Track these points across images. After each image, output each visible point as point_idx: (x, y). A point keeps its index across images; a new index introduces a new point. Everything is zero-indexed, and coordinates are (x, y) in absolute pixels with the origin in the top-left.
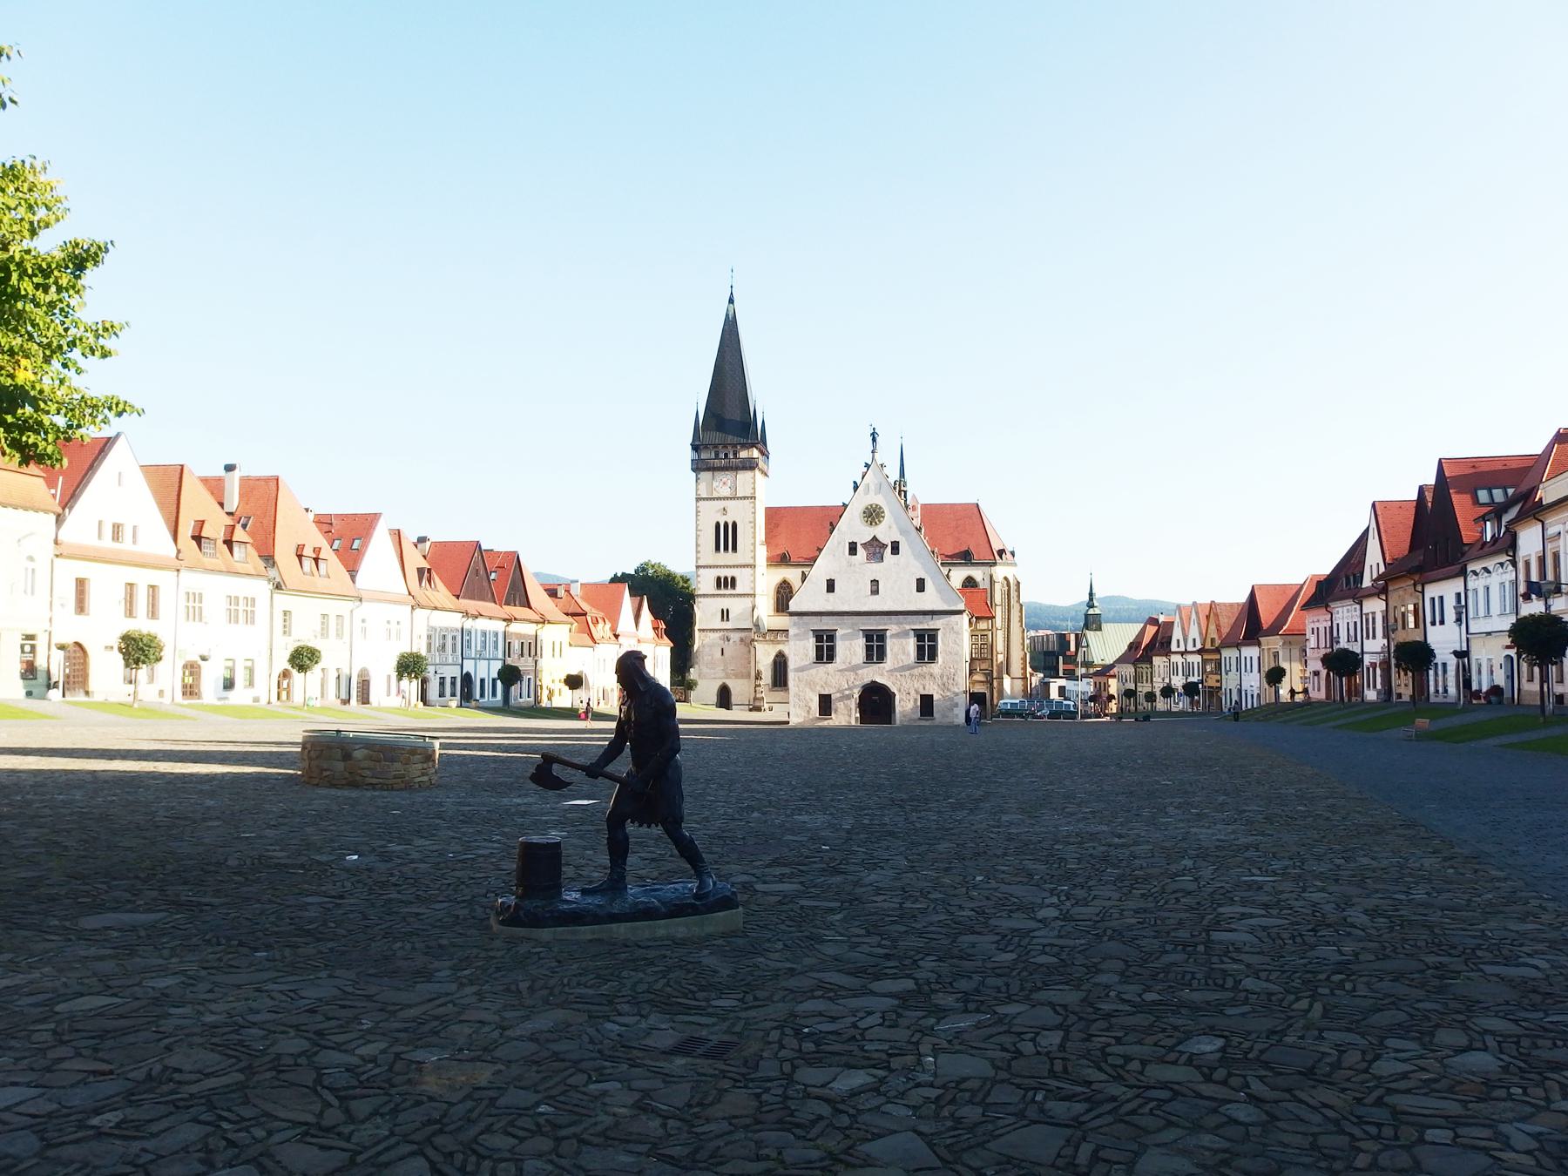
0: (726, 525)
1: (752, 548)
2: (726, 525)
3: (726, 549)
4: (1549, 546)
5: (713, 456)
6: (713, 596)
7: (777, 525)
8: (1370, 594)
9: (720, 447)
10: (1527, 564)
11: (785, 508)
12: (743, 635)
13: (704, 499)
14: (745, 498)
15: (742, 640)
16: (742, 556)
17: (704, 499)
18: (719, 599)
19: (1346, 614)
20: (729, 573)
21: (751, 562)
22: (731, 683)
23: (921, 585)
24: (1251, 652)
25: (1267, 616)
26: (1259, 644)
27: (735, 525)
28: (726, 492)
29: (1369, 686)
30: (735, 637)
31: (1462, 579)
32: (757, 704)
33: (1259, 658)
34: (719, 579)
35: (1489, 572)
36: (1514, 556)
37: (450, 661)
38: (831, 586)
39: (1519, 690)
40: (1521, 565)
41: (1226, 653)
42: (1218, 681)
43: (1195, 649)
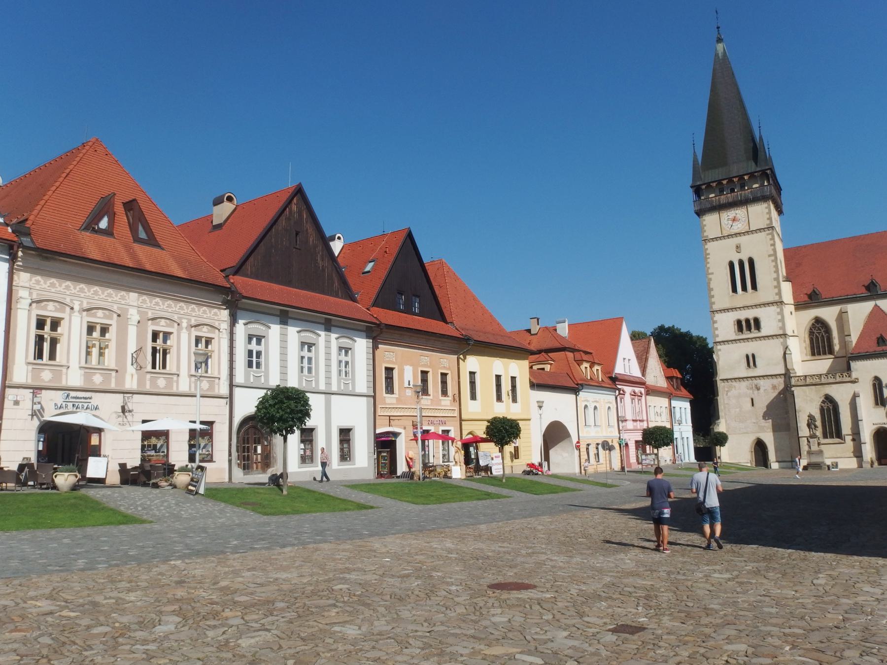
1: (775, 283)
2: (741, 263)
3: (744, 288)
6: (735, 340)
9: (725, 182)
11: (805, 247)
13: (716, 239)
14: (760, 230)
15: (774, 387)
16: (766, 291)
17: (716, 239)
18: (742, 344)
20: (750, 314)
21: (777, 298)
27: (751, 262)
28: (738, 227)
30: (764, 384)
32: (815, 459)
34: (739, 322)
37: (184, 385)
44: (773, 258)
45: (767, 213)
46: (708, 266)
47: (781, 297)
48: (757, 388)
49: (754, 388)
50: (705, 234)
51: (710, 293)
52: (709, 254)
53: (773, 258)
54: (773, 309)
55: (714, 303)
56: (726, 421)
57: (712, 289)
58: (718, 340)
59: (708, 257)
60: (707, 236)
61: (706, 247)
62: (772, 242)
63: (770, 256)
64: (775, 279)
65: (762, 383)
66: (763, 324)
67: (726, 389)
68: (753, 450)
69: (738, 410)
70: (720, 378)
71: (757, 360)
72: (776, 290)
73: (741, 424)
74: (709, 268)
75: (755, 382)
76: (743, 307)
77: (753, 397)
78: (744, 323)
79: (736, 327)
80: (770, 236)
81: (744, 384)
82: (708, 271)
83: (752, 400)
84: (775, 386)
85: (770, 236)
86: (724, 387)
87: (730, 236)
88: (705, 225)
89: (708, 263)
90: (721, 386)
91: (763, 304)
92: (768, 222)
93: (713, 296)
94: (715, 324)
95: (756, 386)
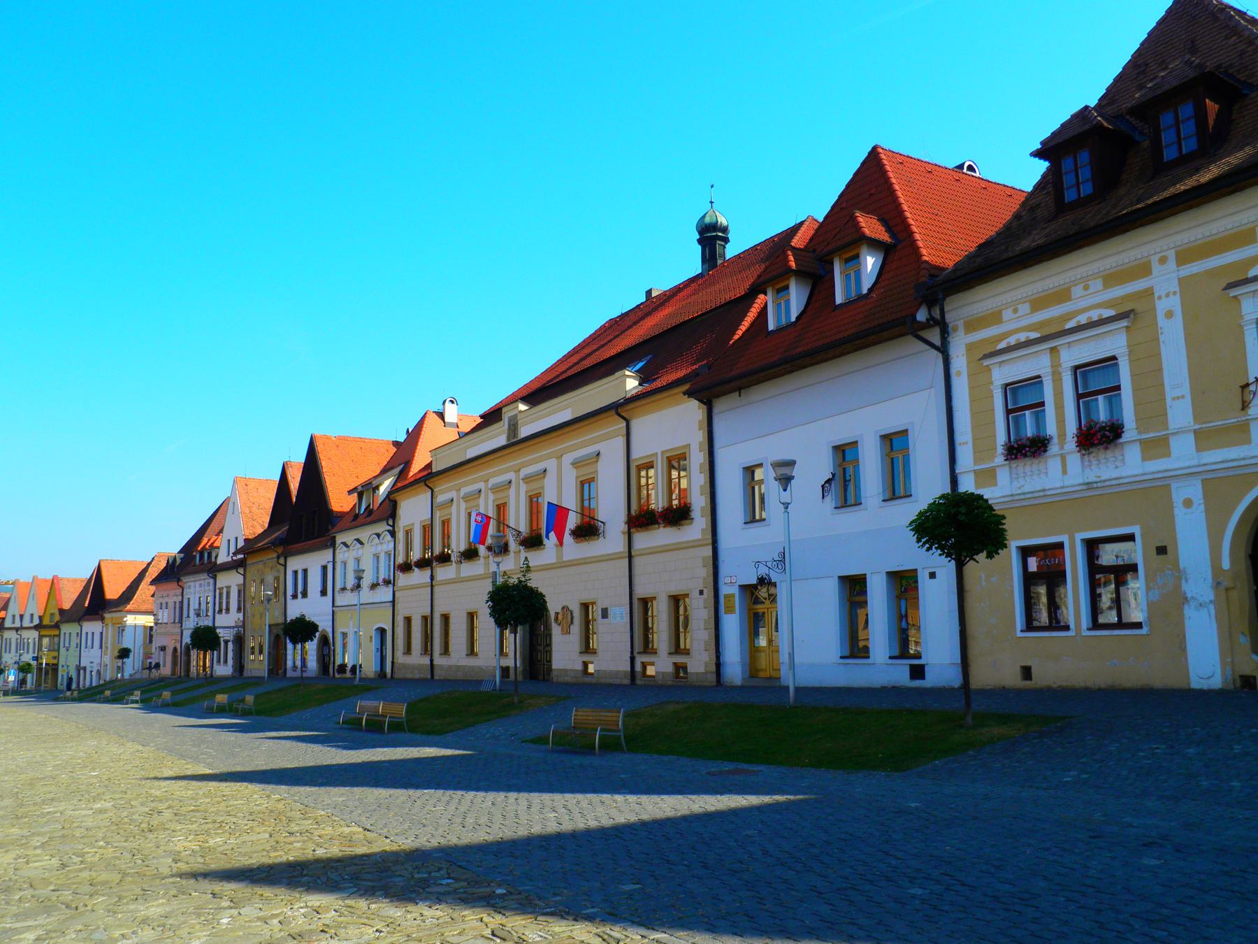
4: (438, 514)
8: (227, 567)
10: (408, 533)
19: (198, 588)
24: (93, 627)
25: (113, 590)
26: (102, 619)
29: (219, 661)
31: (331, 550)
33: (102, 633)
35: (361, 543)
36: (393, 526)
39: (393, 663)
40: (400, 535)
41: (67, 629)
42: (55, 658)
43: (32, 625)
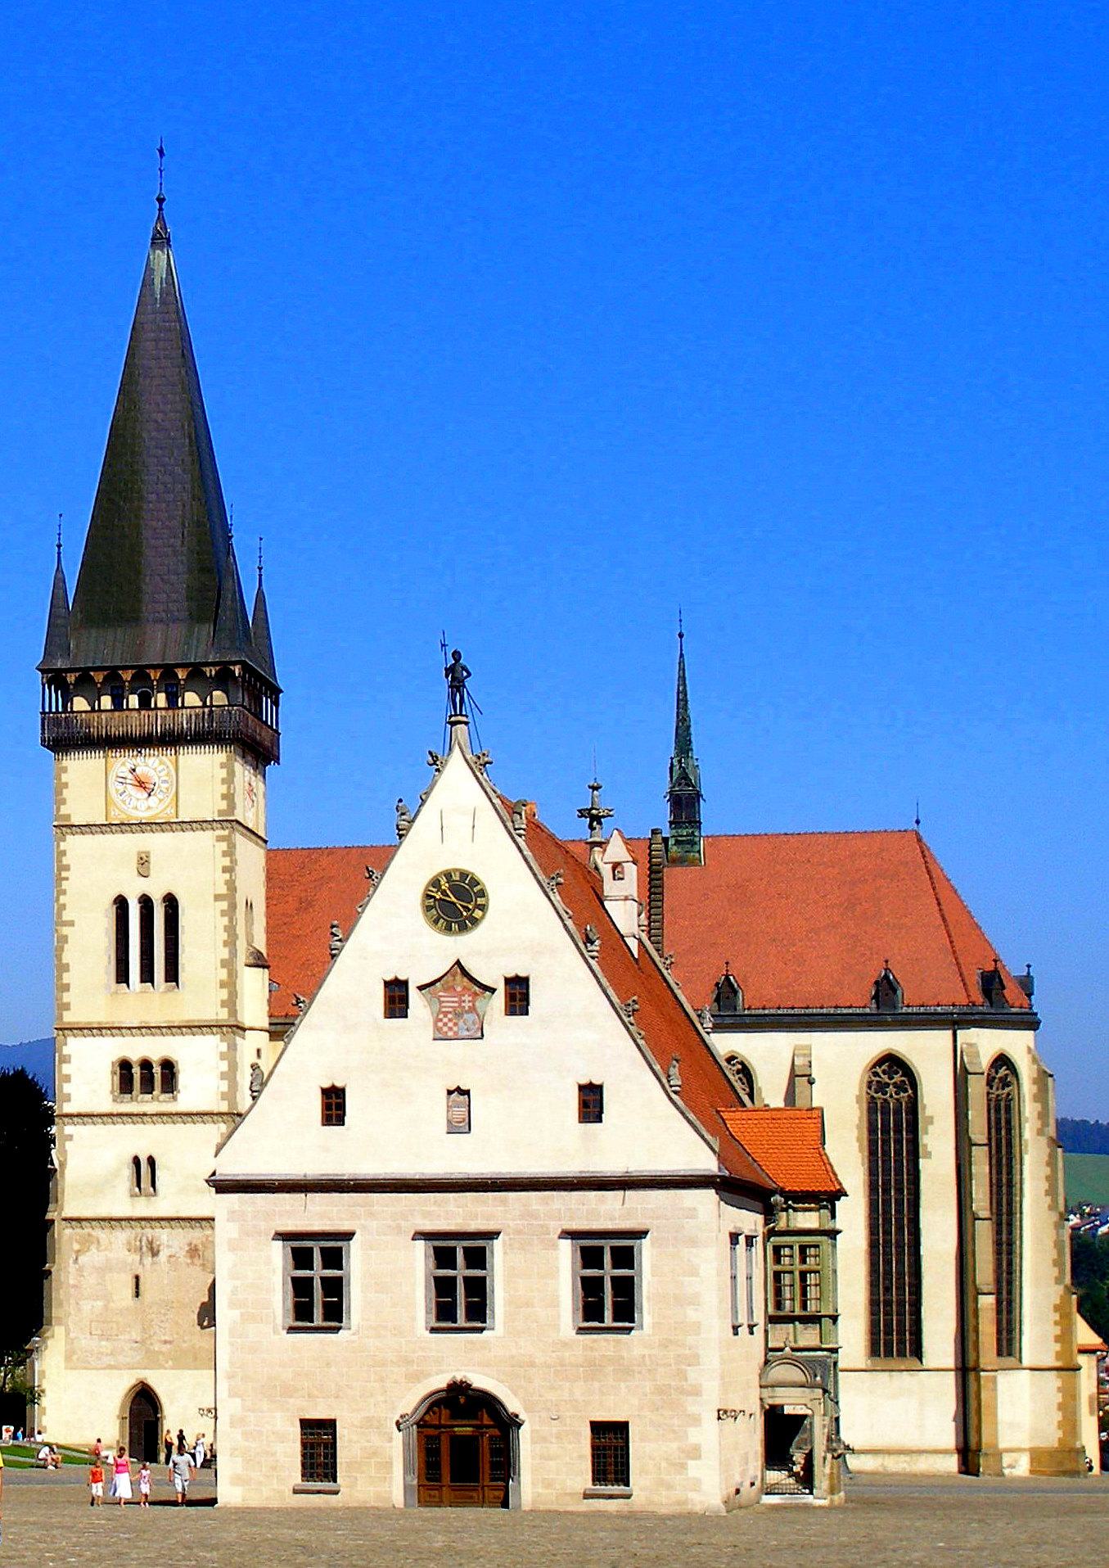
0: (146, 903)
1: (223, 974)
2: (146, 903)
3: (147, 976)
5: (106, 702)
7: (305, 905)
11: (330, 851)
12: (196, 1235)
15: (193, 1252)
18: (129, 1127)
20: (154, 1049)
21: (223, 1015)
22: (160, 1384)
23: (591, 1103)
27: (171, 902)
30: (172, 1240)
38: (334, 1106)
44: (224, 905)
45: (223, 781)
46: (62, 899)
47: (233, 1012)
48: (152, 1249)
49: (144, 1249)
50: (64, 810)
51: (60, 977)
52: (67, 868)
53: (224, 905)
54: (212, 1043)
55: (67, 1007)
56: (68, 1332)
57: (66, 968)
58: (68, 1108)
59: (64, 874)
60: (68, 817)
61: (63, 846)
62: (226, 862)
63: (218, 898)
64: (225, 964)
65: (163, 1235)
66: (182, 1080)
67: (76, 1247)
68: (127, 1415)
69: (100, 1303)
70: (64, 1215)
71: (158, 1173)
72: (224, 994)
73: (103, 1343)
74: (63, 907)
75: (149, 1232)
76: (139, 1028)
77: (139, 1272)
78: (136, 1071)
79: (117, 1078)
80: (224, 846)
81: (122, 1236)
82: (60, 915)
83: (137, 1278)
84: (196, 1250)
85: (224, 846)
86: (71, 1238)
87: (124, 827)
88: (66, 785)
89: (64, 892)
90: (65, 1238)
91: (189, 1027)
92: (223, 805)
93: (66, 988)
94: (64, 1066)
95: (151, 1243)
